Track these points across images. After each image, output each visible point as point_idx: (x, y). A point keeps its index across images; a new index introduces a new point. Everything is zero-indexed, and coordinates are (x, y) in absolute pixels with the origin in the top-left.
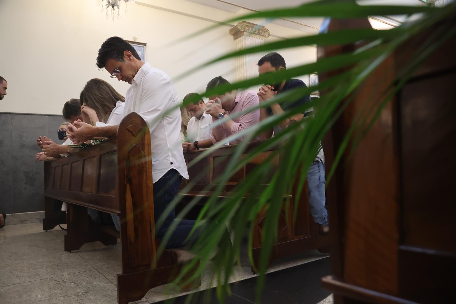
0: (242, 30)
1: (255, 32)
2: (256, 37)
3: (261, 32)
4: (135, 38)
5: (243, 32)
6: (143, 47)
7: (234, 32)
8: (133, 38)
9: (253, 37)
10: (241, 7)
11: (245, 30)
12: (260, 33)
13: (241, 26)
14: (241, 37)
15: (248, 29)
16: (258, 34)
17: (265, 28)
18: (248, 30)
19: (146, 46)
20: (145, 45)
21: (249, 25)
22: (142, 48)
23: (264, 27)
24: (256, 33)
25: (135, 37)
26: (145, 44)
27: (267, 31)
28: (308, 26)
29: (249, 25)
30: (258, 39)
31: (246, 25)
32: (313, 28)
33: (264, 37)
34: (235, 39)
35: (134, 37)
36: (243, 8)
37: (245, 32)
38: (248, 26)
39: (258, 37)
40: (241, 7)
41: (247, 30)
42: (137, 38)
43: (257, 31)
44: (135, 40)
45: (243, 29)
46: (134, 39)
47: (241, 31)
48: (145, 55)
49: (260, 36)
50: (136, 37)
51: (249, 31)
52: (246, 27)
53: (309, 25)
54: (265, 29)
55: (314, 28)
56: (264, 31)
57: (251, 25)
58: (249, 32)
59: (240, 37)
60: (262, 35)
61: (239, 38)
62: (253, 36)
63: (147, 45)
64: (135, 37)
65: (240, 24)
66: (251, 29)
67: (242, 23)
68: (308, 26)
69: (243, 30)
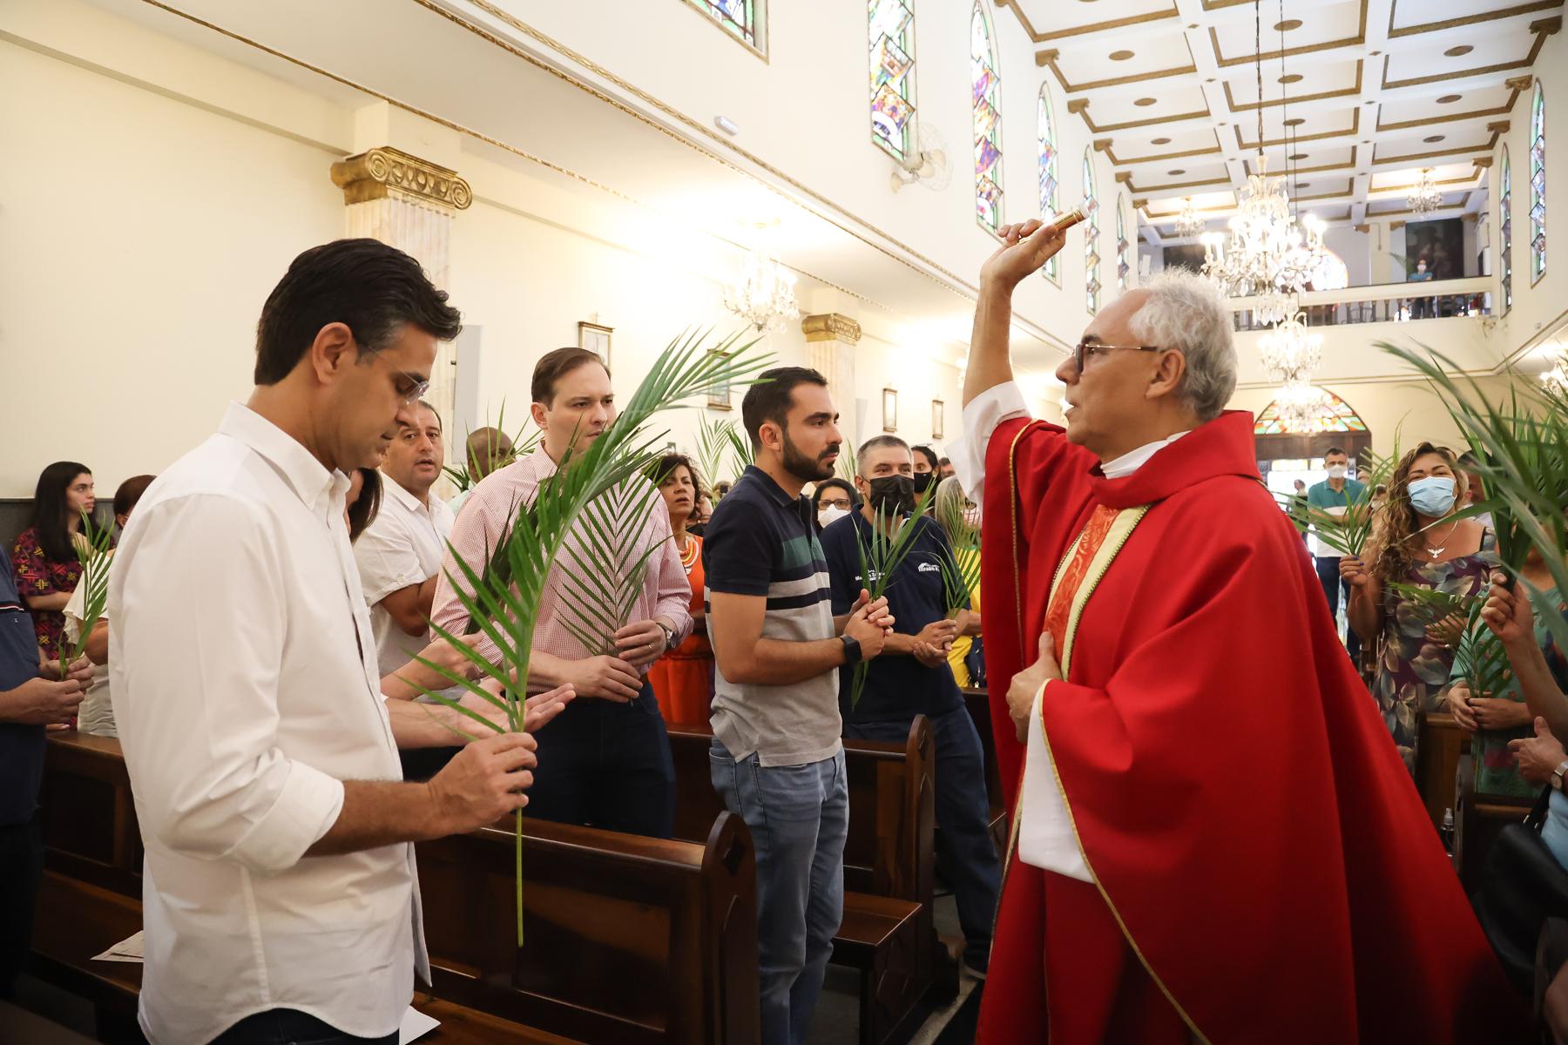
0: (380, 177)
1: (424, 186)
2: (425, 204)
3: (444, 190)
5: (386, 182)
7: (348, 177)
9: (417, 206)
10: (384, 98)
11: (392, 179)
12: (441, 191)
13: (377, 162)
14: (376, 203)
15: (400, 175)
16: (434, 195)
17: (457, 175)
18: (402, 179)
21: (403, 161)
23: (456, 172)
24: (427, 190)
27: (463, 187)
28: (591, 183)
29: (403, 161)
30: (434, 212)
31: (394, 161)
32: (603, 187)
33: (452, 206)
34: (352, 200)
36: (387, 102)
37: (390, 185)
38: (402, 164)
39: (435, 208)
40: (384, 98)
41: (399, 180)
43: (432, 185)
45: (384, 174)
47: (379, 182)
49: (440, 203)
51: (405, 184)
52: (394, 167)
53: (592, 181)
54: (456, 180)
55: (607, 190)
56: (454, 186)
57: (412, 163)
58: (405, 189)
59: (372, 198)
60: (446, 199)
61: (365, 201)
62: (417, 201)
65: (375, 157)
66: (410, 178)
67: (382, 152)
68: (591, 183)
69: (383, 179)
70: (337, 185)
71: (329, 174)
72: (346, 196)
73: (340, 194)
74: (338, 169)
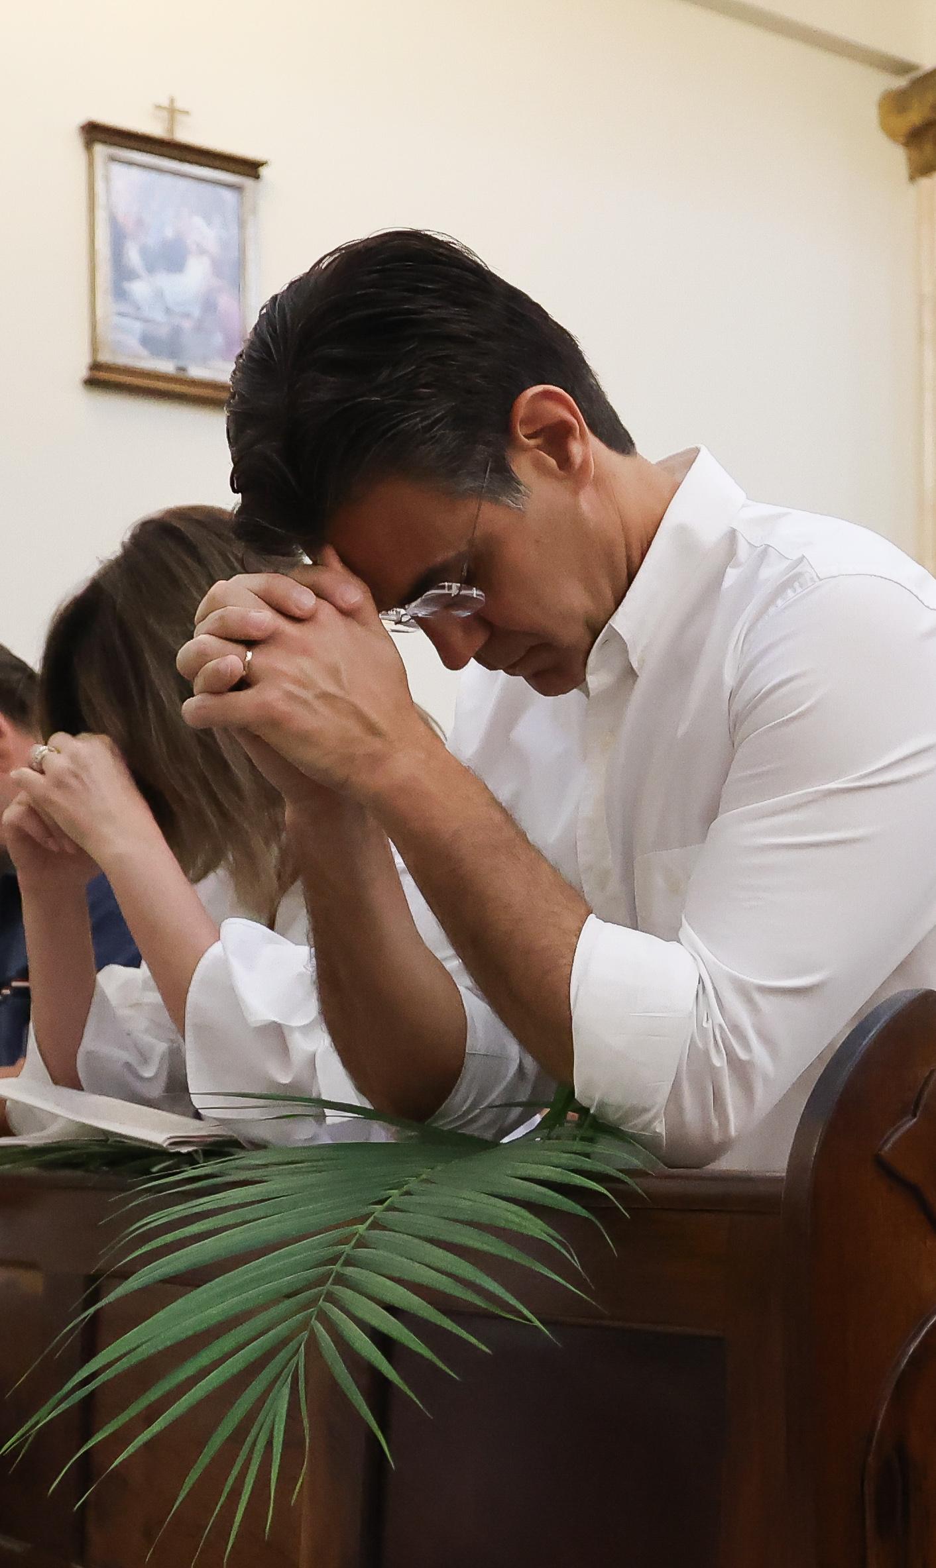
4: (172, 112)
6: (237, 188)
7: (915, 117)
8: (159, 107)
19: (257, 177)
20: (248, 175)
22: (228, 196)
25: (172, 101)
26: (250, 168)
35: (165, 103)
42: (187, 113)
44: (171, 130)
46: (165, 114)
48: (251, 254)
50: (179, 105)
63: (263, 171)
64: (172, 101)
70: (891, 134)
71: (872, 114)
72: (909, 159)
73: (897, 157)
74: (895, 103)
